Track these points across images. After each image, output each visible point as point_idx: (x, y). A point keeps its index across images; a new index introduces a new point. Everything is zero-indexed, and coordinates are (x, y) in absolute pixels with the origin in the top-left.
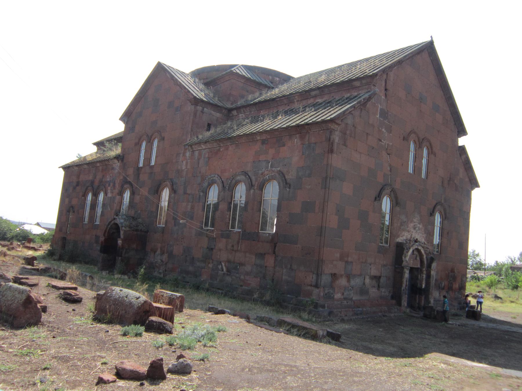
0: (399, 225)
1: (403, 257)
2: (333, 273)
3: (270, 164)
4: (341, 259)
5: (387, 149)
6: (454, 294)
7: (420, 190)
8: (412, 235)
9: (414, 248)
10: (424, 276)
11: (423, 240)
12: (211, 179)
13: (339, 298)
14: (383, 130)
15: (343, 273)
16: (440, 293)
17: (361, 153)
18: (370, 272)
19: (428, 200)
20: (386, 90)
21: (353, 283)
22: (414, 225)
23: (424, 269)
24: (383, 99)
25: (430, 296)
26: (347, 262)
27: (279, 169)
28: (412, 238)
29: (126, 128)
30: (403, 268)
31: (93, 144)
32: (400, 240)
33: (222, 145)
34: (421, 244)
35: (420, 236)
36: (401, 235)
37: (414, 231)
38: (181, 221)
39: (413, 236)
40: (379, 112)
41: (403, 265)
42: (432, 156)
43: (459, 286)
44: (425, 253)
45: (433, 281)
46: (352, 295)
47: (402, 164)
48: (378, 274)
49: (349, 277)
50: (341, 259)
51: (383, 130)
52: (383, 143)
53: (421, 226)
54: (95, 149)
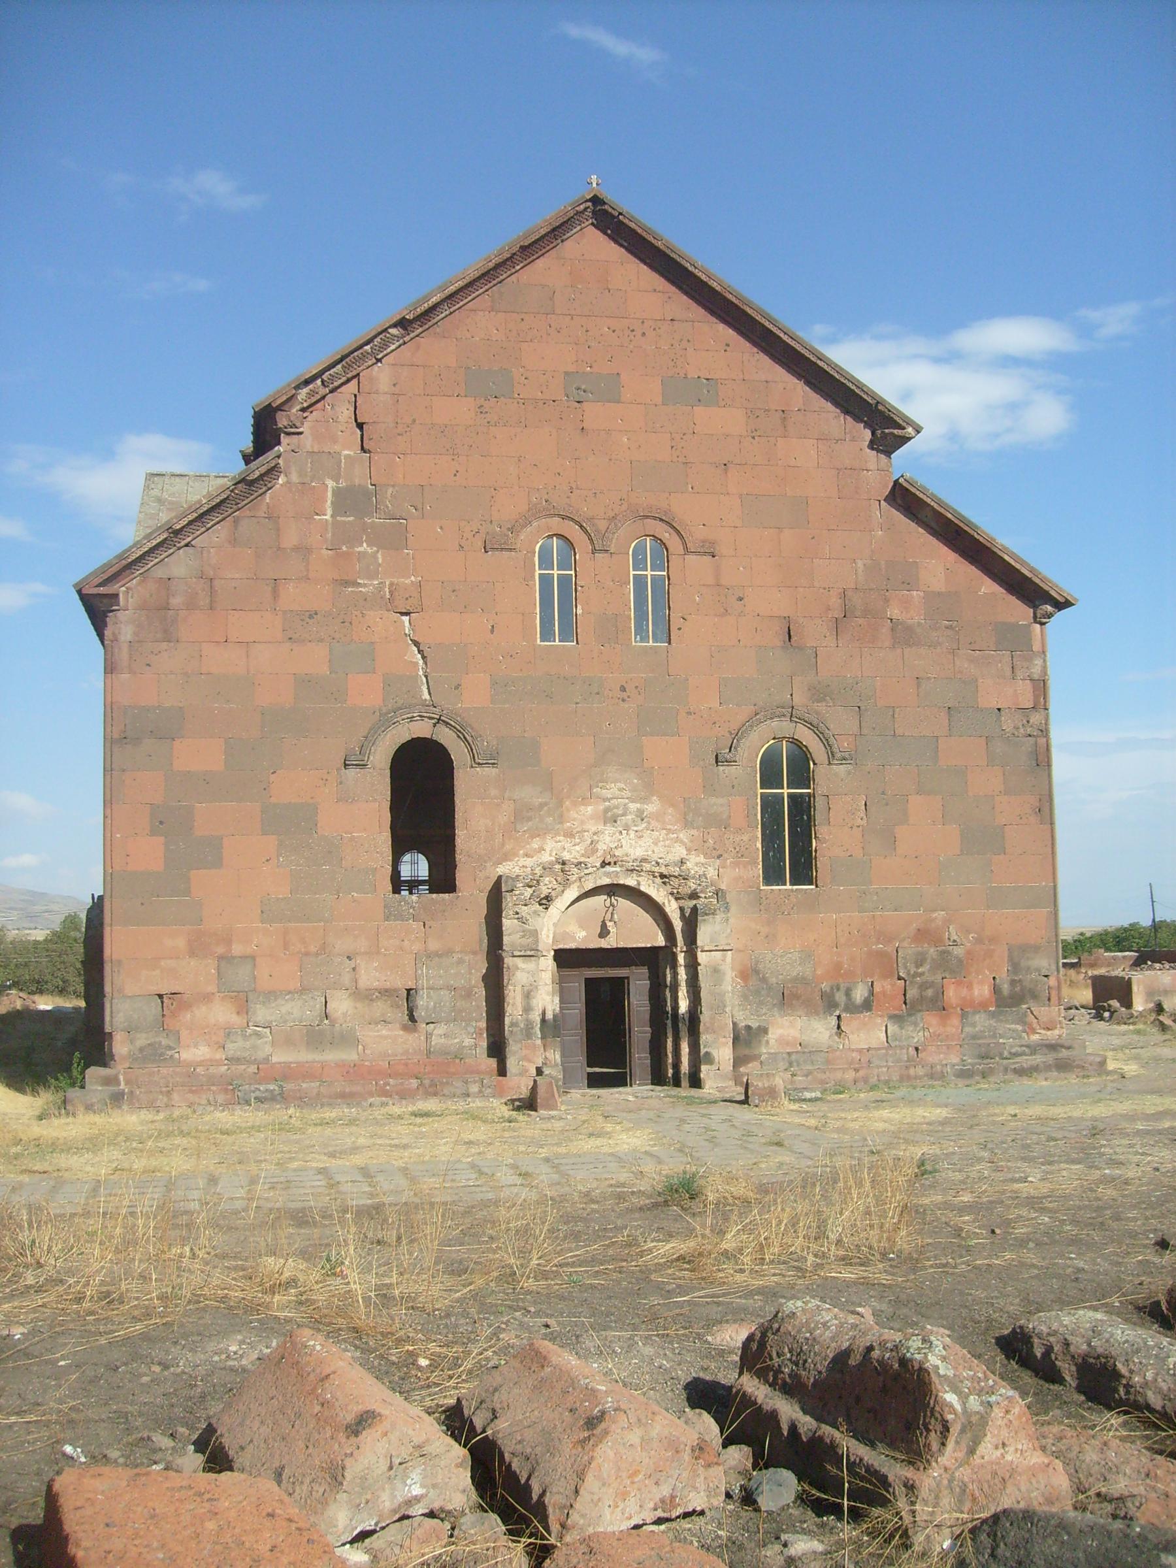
0: (503, 818)
6: (955, 1021)
7: (623, 689)
9: (589, 886)
11: (680, 851)
13: (202, 1058)
15: (212, 988)
16: (839, 1027)
19: (689, 713)
20: (360, 426)
21: (262, 1013)
22: (607, 810)
24: (347, 457)
25: (704, 1038)
28: (600, 853)
32: (501, 870)
34: (647, 866)
37: (609, 829)
39: (601, 847)
40: (332, 503)
41: (504, 948)
43: (996, 990)
46: (268, 1049)
48: (401, 983)
52: (365, 585)
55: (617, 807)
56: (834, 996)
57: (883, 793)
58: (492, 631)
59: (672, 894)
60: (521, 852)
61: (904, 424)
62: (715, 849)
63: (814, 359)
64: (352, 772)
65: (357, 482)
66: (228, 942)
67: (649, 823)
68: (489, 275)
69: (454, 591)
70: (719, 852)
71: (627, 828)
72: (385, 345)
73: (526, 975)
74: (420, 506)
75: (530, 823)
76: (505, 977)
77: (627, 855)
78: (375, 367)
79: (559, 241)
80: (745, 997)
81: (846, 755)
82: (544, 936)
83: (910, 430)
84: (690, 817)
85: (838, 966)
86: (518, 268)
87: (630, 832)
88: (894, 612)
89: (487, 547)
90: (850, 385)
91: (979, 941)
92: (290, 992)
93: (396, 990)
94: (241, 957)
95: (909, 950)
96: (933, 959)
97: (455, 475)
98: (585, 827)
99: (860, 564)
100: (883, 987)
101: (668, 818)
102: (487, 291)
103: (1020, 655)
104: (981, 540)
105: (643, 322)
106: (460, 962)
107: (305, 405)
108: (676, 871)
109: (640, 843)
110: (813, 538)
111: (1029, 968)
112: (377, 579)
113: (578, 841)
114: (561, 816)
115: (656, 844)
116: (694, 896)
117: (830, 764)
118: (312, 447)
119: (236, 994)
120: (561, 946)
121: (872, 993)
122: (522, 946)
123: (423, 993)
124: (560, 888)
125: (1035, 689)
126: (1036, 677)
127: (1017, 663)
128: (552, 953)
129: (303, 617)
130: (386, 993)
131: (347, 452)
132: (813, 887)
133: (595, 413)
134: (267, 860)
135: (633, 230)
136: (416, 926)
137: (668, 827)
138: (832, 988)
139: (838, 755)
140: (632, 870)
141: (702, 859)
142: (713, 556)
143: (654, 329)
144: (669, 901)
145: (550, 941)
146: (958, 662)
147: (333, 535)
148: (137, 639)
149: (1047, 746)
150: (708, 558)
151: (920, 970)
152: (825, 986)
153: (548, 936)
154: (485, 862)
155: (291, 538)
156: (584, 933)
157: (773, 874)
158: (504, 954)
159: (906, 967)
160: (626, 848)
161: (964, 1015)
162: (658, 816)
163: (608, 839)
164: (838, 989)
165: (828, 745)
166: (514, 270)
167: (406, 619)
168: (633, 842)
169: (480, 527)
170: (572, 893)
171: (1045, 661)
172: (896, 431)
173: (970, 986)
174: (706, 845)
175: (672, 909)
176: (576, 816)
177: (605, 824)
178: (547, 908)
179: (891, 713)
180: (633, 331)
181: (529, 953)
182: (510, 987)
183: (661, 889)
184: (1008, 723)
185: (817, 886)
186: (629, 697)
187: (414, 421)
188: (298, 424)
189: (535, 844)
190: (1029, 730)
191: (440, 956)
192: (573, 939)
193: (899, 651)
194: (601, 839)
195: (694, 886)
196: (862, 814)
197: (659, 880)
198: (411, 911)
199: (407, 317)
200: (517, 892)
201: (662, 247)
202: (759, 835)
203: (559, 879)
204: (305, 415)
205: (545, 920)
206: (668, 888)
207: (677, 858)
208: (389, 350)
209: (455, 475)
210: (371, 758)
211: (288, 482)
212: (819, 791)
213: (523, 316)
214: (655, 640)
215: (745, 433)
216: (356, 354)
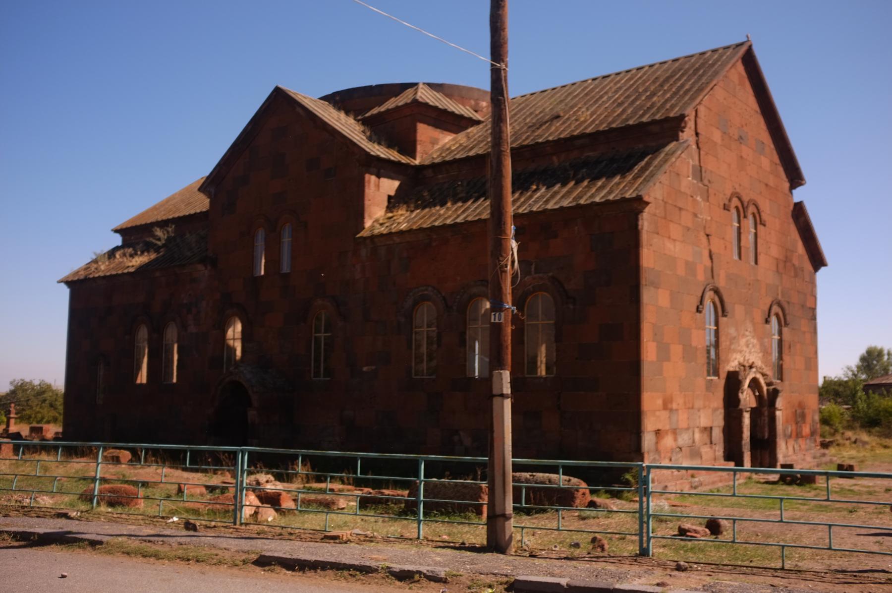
0: (728, 343)
1: (740, 394)
3: (533, 267)
4: (665, 407)
5: (705, 227)
8: (745, 357)
10: (766, 419)
12: (420, 293)
14: (699, 198)
15: (667, 427)
17: (674, 240)
18: (700, 423)
20: (697, 134)
22: (747, 341)
26: (671, 410)
27: (550, 274)
29: (211, 203)
30: (740, 412)
31: (112, 230)
33: (435, 237)
35: (755, 357)
36: (732, 359)
38: (365, 369)
39: (747, 358)
41: (741, 407)
42: (760, 227)
43: (810, 429)
44: (765, 383)
48: (708, 425)
49: (675, 432)
50: (665, 407)
51: (699, 198)
53: (755, 341)
54: (118, 240)
64: (698, 314)
66: (671, 402)
123: (714, 428)
130: (705, 428)
132: (779, 381)
133: (746, 151)
142: (764, 225)
175: (765, 388)
189: (734, 356)
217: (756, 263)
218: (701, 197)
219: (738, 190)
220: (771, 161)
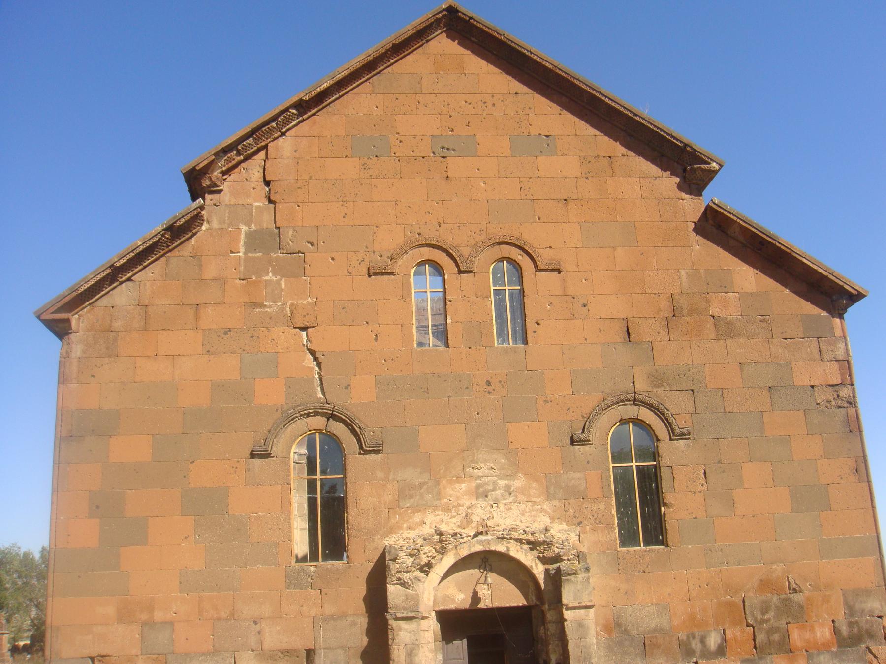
0: (388, 498)
2: (94, 654)
7: (489, 383)
9: (464, 553)
11: (545, 521)
14: (270, 276)
19: (546, 402)
20: (267, 183)
22: (478, 487)
23: (547, 606)
24: (257, 207)
26: (149, 624)
28: (474, 524)
32: (387, 542)
34: (515, 535)
37: (481, 502)
39: (475, 519)
40: (245, 243)
41: (389, 610)
43: (836, 631)
45: (583, 637)
47: (376, 336)
52: (270, 307)
55: (487, 484)
56: (690, 644)
57: (719, 462)
58: (376, 340)
59: (538, 558)
60: (405, 525)
61: (709, 160)
62: (575, 517)
63: (631, 115)
64: (257, 462)
65: (265, 226)
67: (516, 496)
68: (370, 67)
69: (343, 308)
70: (580, 519)
71: (497, 502)
72: (287, 121)
73: (408, 634)
74: (315, 243)
75: (412, 501)
76: (390, 637)
77: (498, 525)
78: (281, 139)
79: (424, 41)
80: (609, 648)
81: (684, 431)
82: (425, 599)
83: (714, 164)
84: (552, 491)
85: (692, 617)
86: (392, 61)
87: (501, 506)
88: (715, 310)
89: (371, 273)
90: (662, 133)
91: (816, 588)
92: (203, 654)
93: (295, 650)
94: (161, 623)
95: (754, 599)
96: (777, 607)
97: (344, 217)
98: (461, 502)
99: (683, 272)
100: (734, 634)
101: (532, 492)
102: (369, 79)
103: (825, 341)
104: (782, 247)
105: (493, 96)
106: (354, 624)
107: (224, 169)
108: (541, 537)
109: (508, 513)
110: (642, 254)
111: (863, 611)
112: (280, 302)
113: (455, 514)
114: (439, 493)
115: (523, 515)
116: (557, 559)
117: (671, 439)
118: (230, 201)
119: (156, 656)
120: (442, 608)
121: (724, 640)
122: (404, 609)
124: (439, 556)
125: (841, 368)
126: (841, 358)
127: (824, 347)
128: (434, 614)
129: (219, 334)
131: (257, 204)
132: (664, 546)
133: (457, 165)
134: (186, 538)
135: (481, 29)
136: (314, 592)
137: (533, 499)
138: (688, 637)
139: (678, 431)
140: (503, 538)
141: (564, 526)
142: (559, 271)
143: (502, 101)
144: (536, 564)
145: (431, 603)
146: (773, 349)
147: (245, 267)
148: (84, 355)
149: (857, 415)
150: (556, 274)
151: (766, 617)
152: (682, 636)
153: (429, 599)
154: (373, 535)
155: (211, 271)
156: (461, 596)
157: (628, 537)
158: (388, 616)
159: (753, 615)
160: (497, 519)
161: (809, 656)
162: (522, 491)
163: (480, 511)
164: (694, 638)
165: (669, 425)
166: (389, 64)
167: (304, 333)
168: (503, 514)
169: (365, 257)
170: (449, 560)
171: (846, 344)
172: (702, 166)
173: (812, 629)
174: (567, 514)
175: (539, 571)
176: (452, 492)
177: (477, 498)
178: (427, 575)
179: (720, 394)
180: (485, 103)
181: (410, 615)
182: (395, 646)
183: (528, 554)
184: (820, 397)
185: (667, 546)
186: (494, 390)
187: (311, 177)
188: (218, 183)
189: (417, 518)
190: (839, 403)
191: (334, 619)
192: (453, 600)
193: (722, 342)
194: (475, 512)
195: (557, 551)
196: (703, 481)
197: (526, 547)
198: (309, 580)
199: (304, 99)
200: (400, 561)
201: (505, 40)
202: (614, 504)
203: (438, 548)
204: (225, 177)
205: (426, 584)
206: (535, 553)
207: (542, 526)
208: (291, 125)
209: (344, 217)
210: (274, 448)
211: (210, 229)
212: (664, 462)
213: (397, 96)
214: (515, 342)
215: (579, 175)
216: (264, 129)
217: (525, 342)
218: (274, 274)
219: (431, 234)
220: (583, 159)
